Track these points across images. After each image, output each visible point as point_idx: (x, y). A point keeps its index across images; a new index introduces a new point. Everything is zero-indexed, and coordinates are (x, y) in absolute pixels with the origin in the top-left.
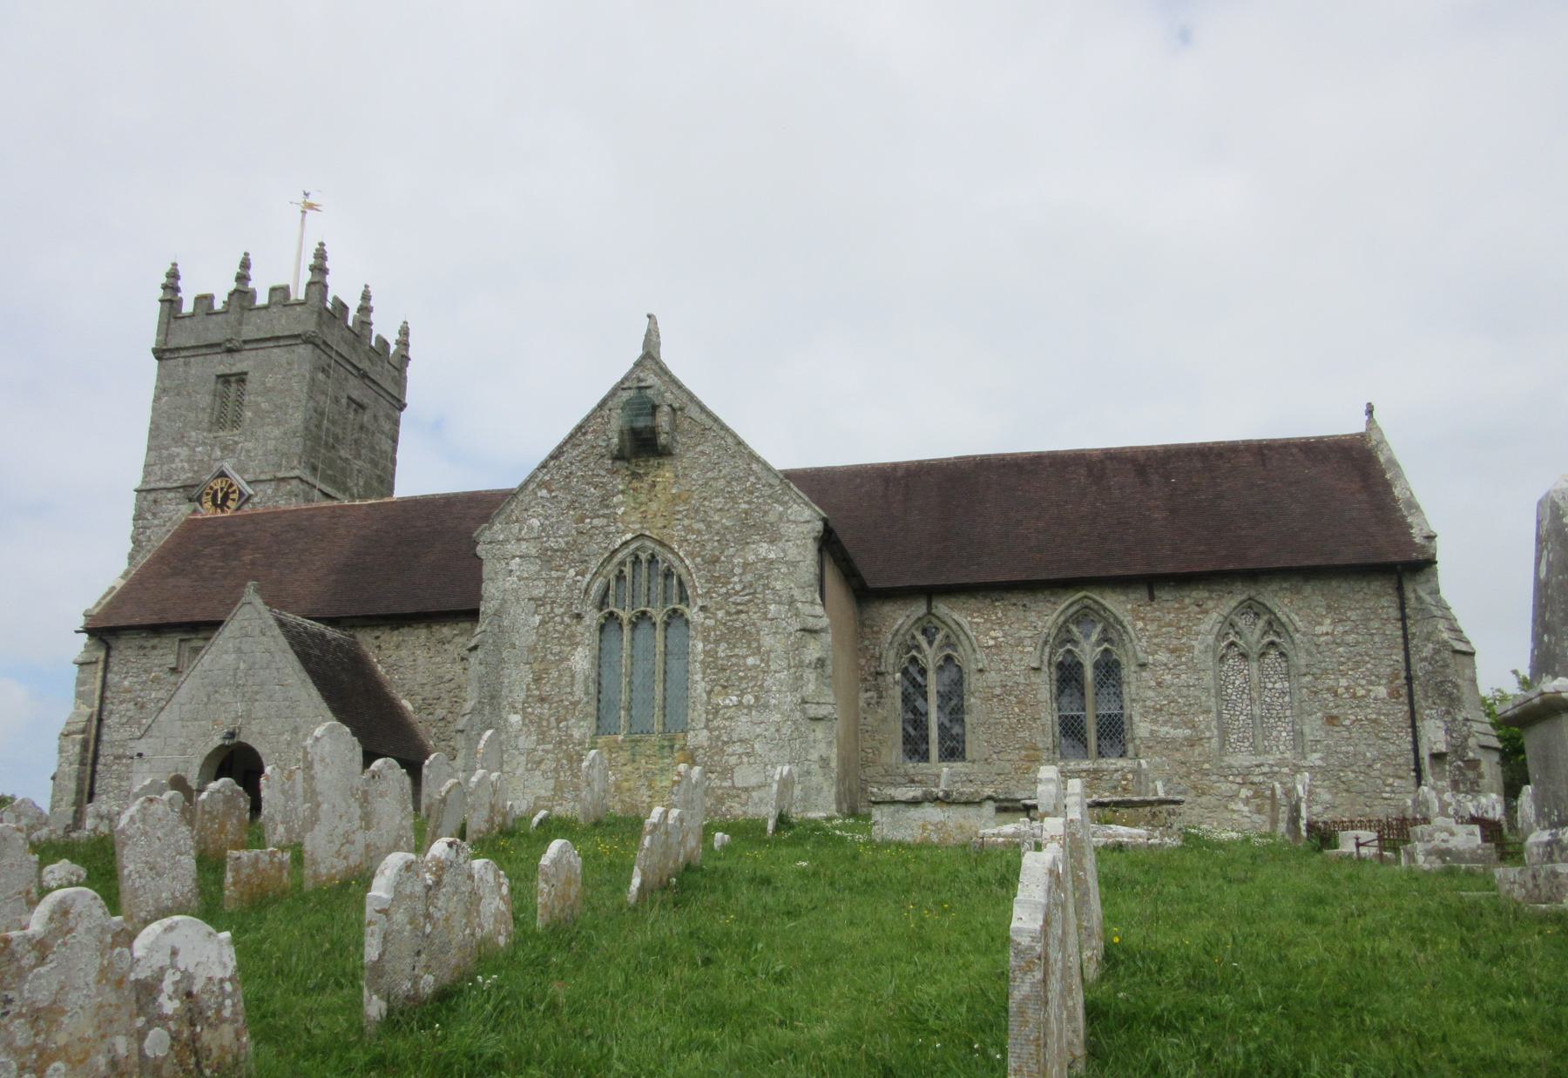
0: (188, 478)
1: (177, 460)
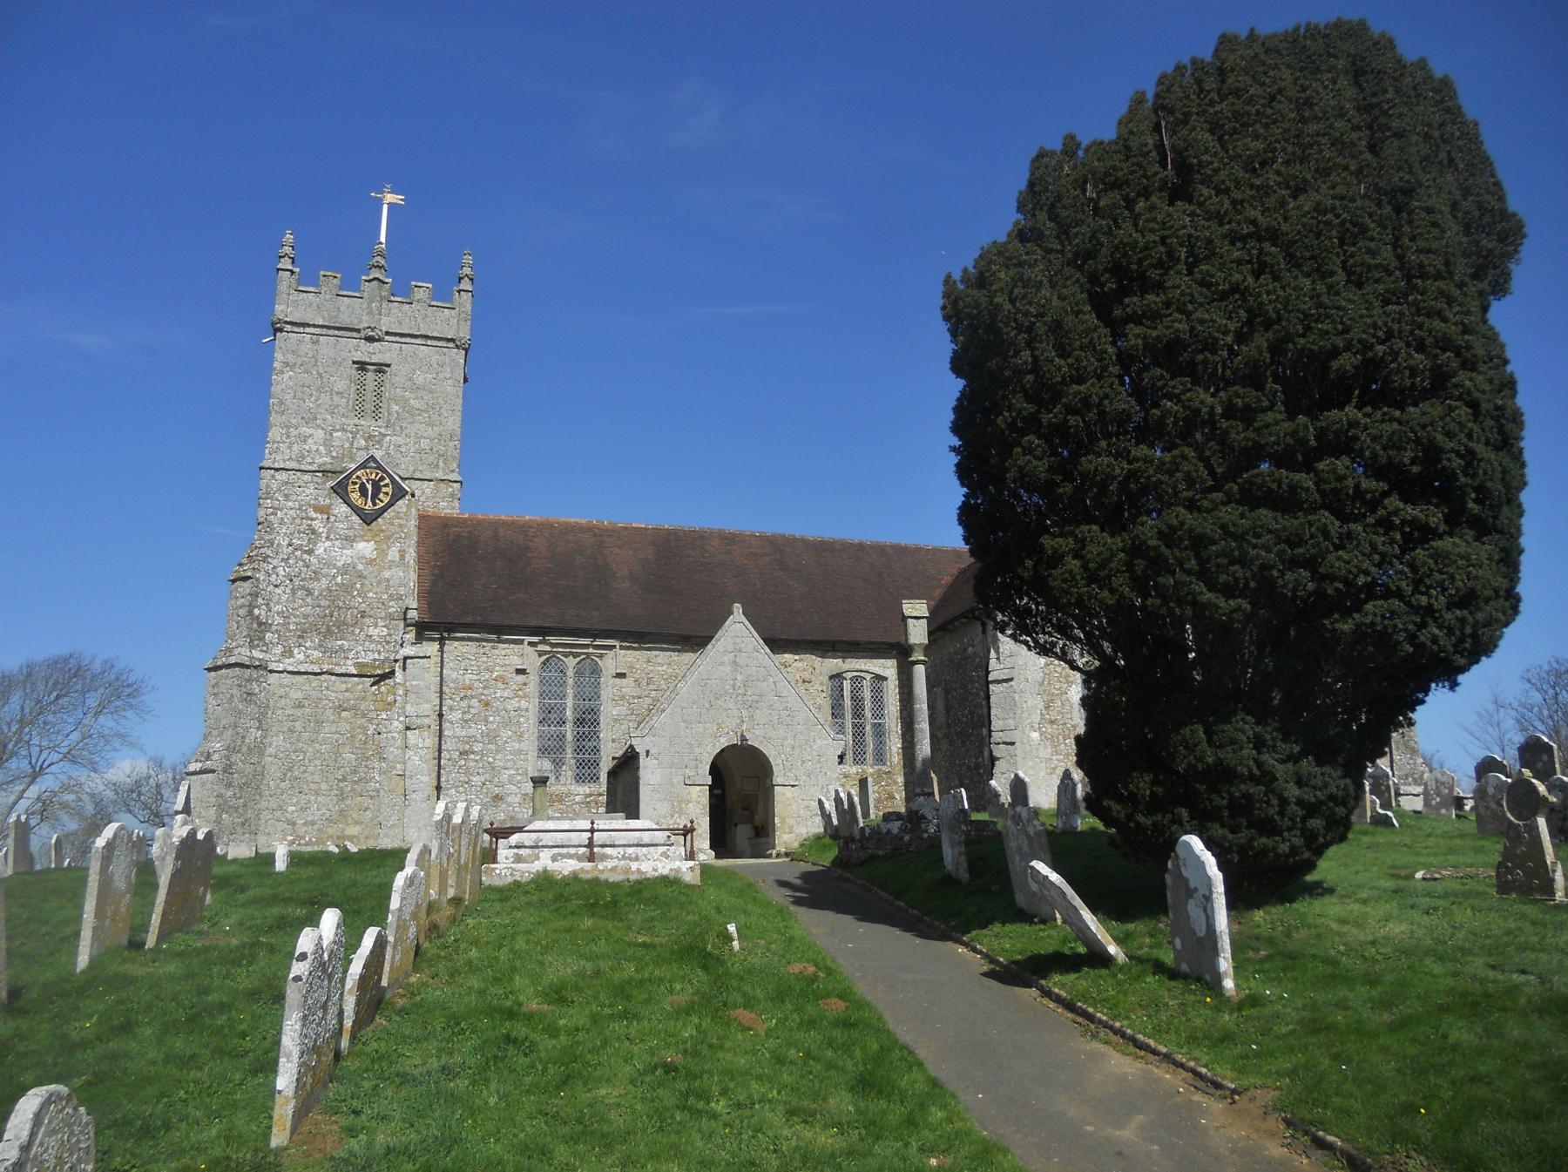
1: (310, 441)
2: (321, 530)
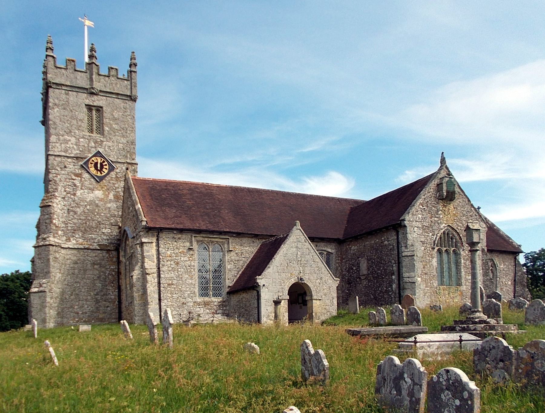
2: (78, 184)
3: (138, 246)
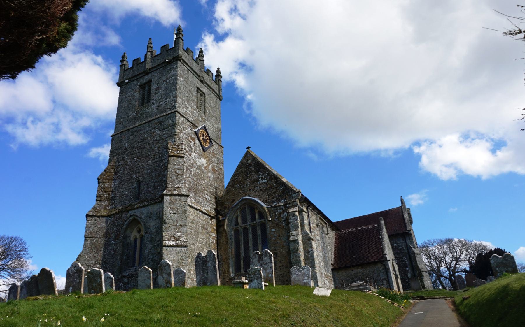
0: (192, 121)
3: (297, 213)
